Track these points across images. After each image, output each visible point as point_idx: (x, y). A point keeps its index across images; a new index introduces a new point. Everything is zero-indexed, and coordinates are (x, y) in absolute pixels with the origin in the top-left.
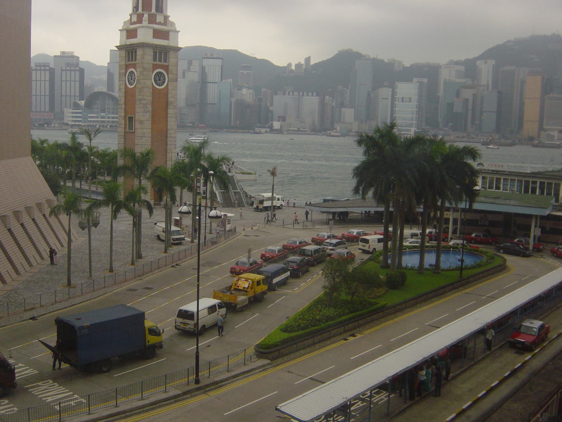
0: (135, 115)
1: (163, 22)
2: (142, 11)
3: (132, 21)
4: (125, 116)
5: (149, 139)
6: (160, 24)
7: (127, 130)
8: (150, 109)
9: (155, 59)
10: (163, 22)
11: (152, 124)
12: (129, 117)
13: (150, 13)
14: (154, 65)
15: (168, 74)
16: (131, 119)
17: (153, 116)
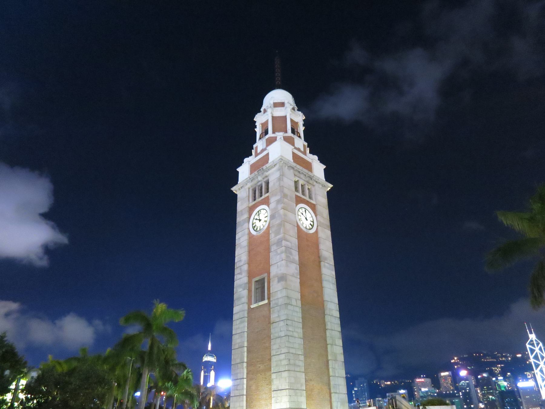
0: (269, 274)
1: (302, 149)
2: (274, 132)
3: (258, 152)
4: (250, 282)
5: (299, 310)
6: (299, 149)
7: (252, 307)
8: (297, 258)
9: (296, 189)
10: (302, 149)
11: (302, 283)
12: (256, 281)
13: (286, 135)
14: (297, 197)
15: (316, 216)
16: (261, 284)
17: (302, 273)
